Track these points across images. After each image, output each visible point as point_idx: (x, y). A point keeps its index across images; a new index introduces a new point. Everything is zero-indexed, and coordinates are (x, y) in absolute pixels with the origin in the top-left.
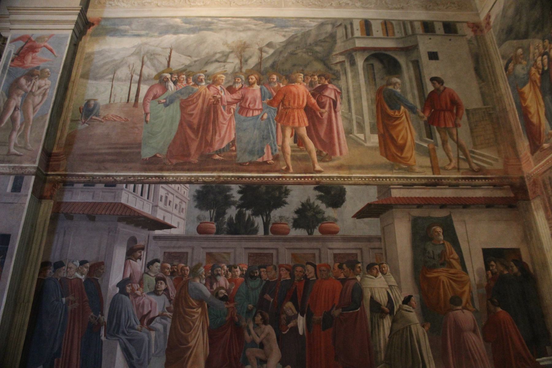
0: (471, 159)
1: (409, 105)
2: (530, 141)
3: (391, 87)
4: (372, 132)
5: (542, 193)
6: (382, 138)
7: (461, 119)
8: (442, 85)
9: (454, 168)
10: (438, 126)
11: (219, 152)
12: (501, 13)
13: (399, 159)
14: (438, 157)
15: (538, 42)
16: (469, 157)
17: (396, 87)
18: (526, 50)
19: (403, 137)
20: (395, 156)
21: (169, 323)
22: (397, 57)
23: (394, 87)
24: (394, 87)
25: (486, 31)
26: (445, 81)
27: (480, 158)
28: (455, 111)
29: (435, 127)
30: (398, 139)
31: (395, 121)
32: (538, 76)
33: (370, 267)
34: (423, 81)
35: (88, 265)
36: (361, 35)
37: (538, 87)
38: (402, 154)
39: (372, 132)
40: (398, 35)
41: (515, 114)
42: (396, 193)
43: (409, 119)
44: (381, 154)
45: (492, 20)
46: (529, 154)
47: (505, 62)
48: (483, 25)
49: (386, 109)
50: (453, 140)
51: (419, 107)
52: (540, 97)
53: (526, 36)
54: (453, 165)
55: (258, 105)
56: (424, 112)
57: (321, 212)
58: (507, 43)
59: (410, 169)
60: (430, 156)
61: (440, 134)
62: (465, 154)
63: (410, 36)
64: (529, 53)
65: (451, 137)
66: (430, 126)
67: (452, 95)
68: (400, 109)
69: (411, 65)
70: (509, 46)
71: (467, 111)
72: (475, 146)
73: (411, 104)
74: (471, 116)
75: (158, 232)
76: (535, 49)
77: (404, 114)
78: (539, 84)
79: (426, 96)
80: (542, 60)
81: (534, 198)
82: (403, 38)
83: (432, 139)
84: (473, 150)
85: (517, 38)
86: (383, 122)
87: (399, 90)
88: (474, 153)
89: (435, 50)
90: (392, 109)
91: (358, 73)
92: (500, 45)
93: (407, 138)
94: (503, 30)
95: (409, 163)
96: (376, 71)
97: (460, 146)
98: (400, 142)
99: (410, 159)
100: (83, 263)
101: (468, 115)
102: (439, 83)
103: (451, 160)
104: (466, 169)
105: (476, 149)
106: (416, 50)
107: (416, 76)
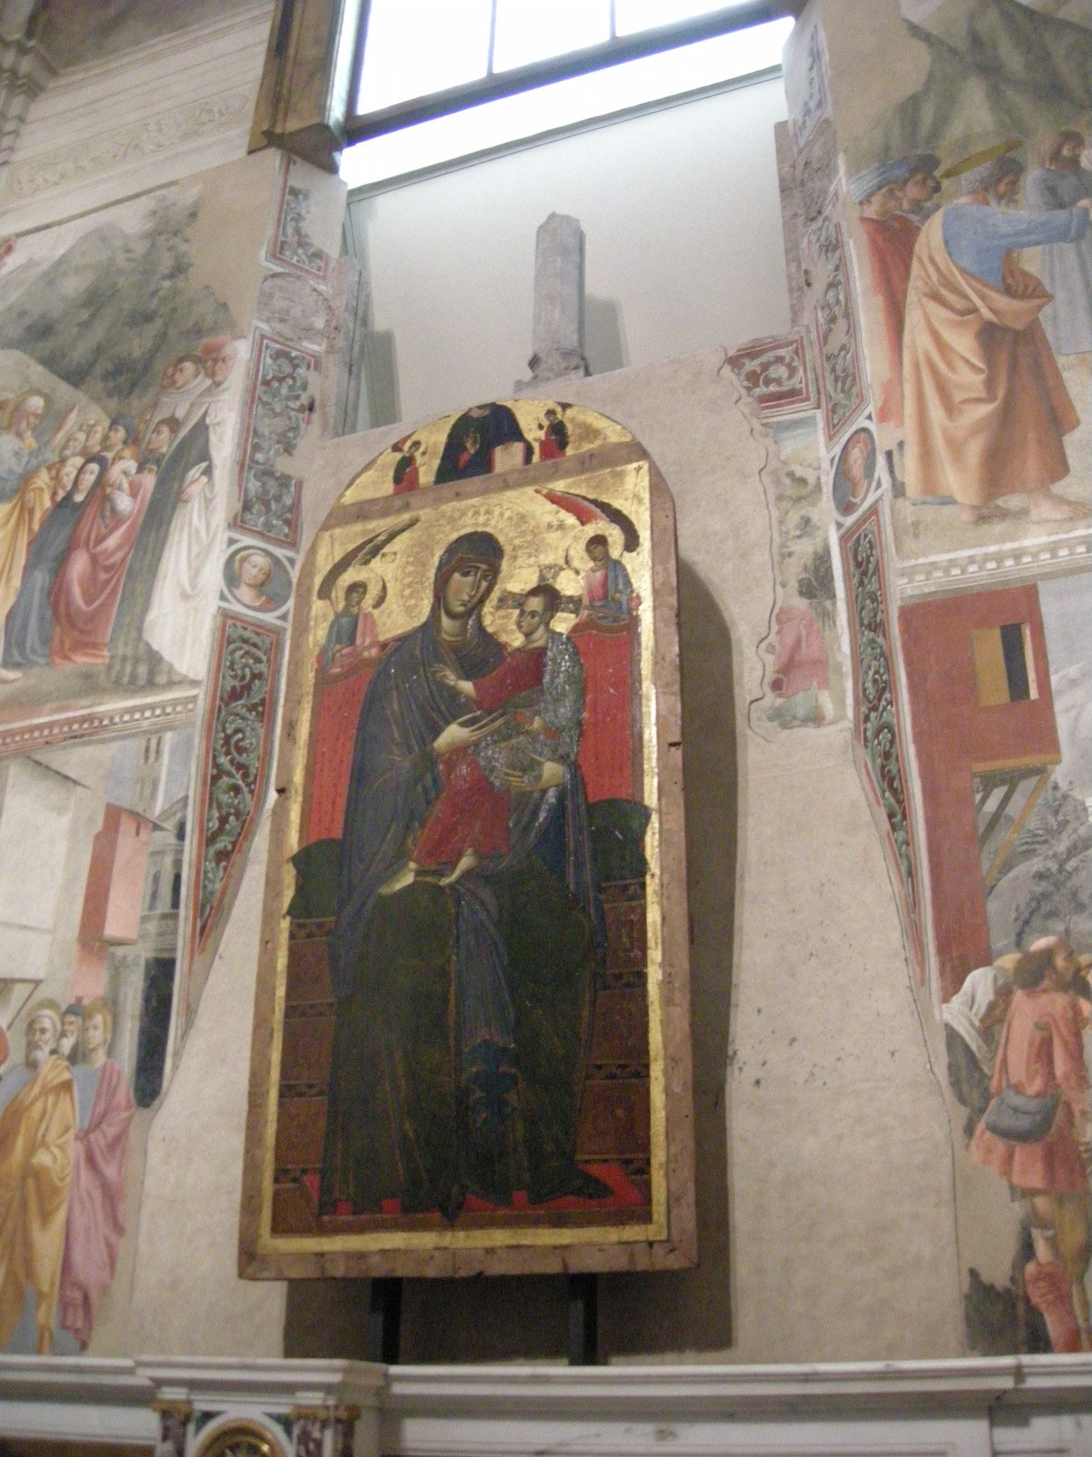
12: (45, 267)
15: (97, 416)
18: (54, 416)
32: (48, 504)
37: (30, 530)
53: (76, 378)
58: (17, 354)
64: (59, 428)
76: (80, 429)
78: (36, 526)
80: (81, 471)
85: (49, 362)
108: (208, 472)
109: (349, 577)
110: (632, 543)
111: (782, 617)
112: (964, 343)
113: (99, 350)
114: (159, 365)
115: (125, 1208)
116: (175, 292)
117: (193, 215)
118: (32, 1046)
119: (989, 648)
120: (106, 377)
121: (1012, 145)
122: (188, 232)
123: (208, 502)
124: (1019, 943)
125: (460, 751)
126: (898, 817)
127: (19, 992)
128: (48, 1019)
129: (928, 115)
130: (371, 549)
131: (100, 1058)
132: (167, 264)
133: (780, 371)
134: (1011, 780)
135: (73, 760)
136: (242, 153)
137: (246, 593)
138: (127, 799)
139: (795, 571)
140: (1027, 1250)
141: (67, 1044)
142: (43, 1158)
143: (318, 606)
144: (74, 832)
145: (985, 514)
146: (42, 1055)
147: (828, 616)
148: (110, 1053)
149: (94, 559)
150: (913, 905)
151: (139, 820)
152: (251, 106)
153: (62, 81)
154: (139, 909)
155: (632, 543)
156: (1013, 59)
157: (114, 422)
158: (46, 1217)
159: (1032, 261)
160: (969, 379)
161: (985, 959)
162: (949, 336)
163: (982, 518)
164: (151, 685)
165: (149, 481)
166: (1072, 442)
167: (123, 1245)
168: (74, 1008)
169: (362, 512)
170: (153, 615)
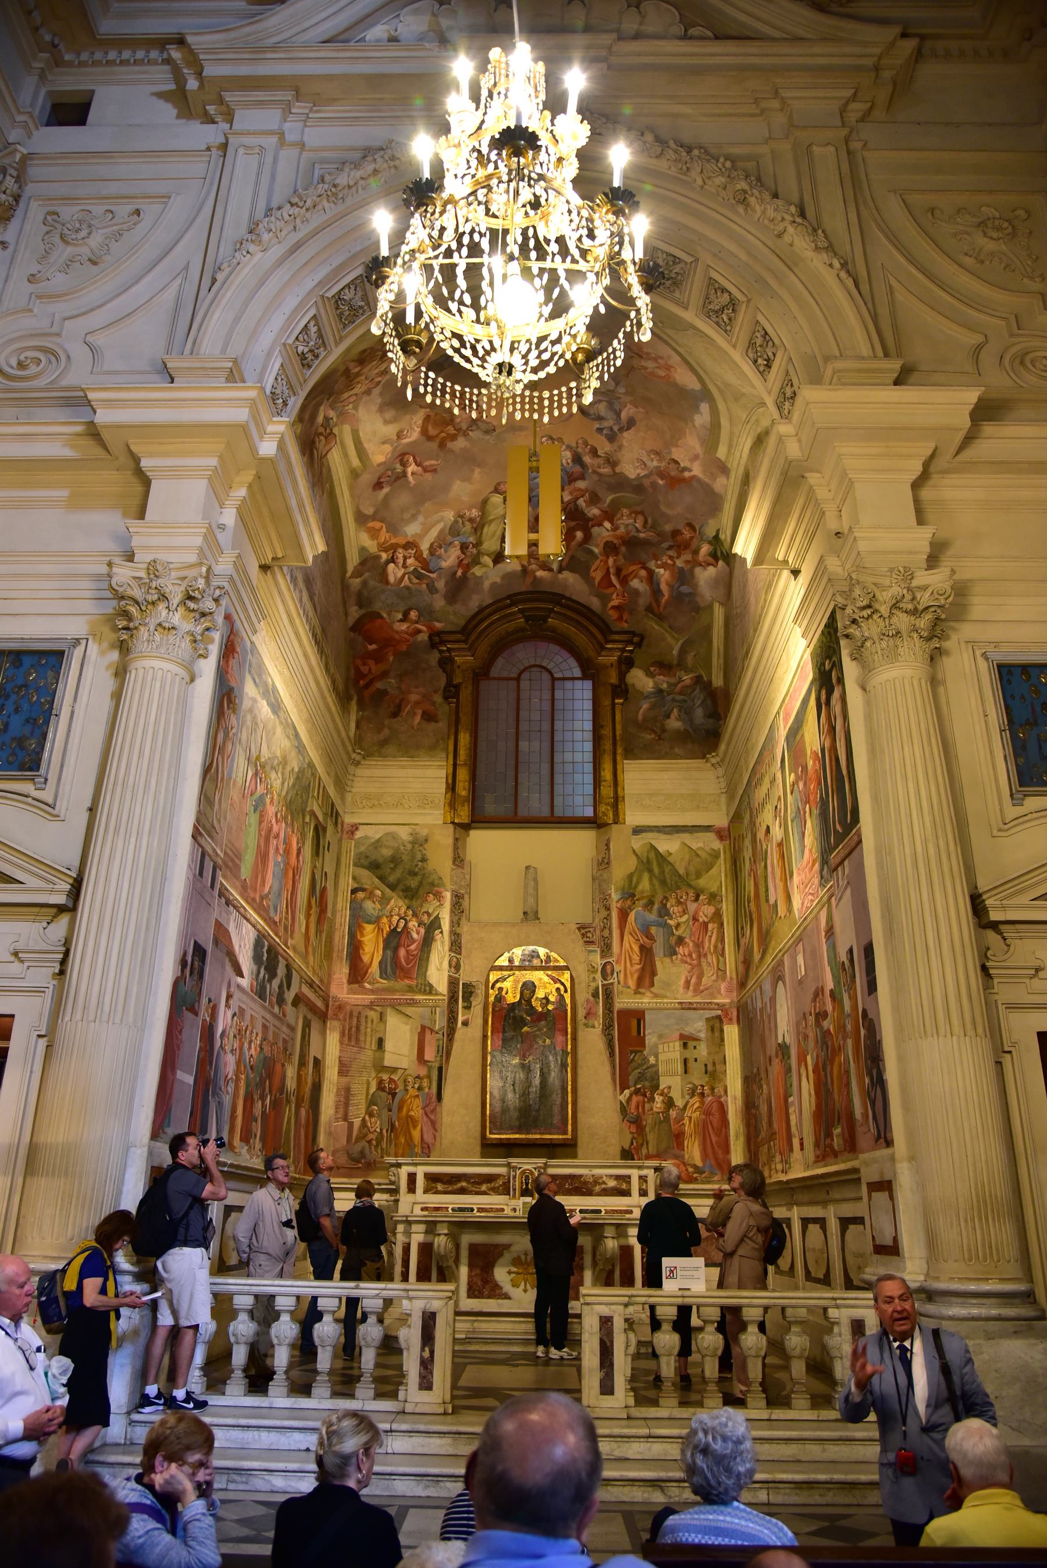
2: (350, 970)
5: (345, 1020)
11: (267, 896)
12: (373, 840)
21: (233, 1085)
25: (345, 836)
33: (290, 1054)
35: (211, 1004)
41: (343, 936)
42: (305, 990)
45: (359, 834)
46: (345, 981)
47: (356, 886)
48: (346, 828)
52: (381, 946)
53: (392, 887)
55: (281, 851)
57: (284, 992)
59: (307, 964)
70: (368, 878)
75: (239, 979)
81: (332, 1019)
85: (382, 878)
92: (355, 865)
94: (367, 857)
100: (210, 1001)
108: (441, 932)
109: (498, 985)
110: (566, 991)
111: (588, 1001)
112: (636, 948)
113: (399, 881)
114: (421, 892)
115: (437, 1126)
116: (424, 868)
117: (426, 840)
118: (406, 1086)
119: (634, 1023)
120: (403, 891)
121: (653, 896)
122: (426, 846)
123: (443, 943)
124: (635, 1085)
125: (528, 1033)
126: (612, 1054)
127: (400, 1072)
128: (410, 1079)
129: (635, 879)
130: (504, 979)
131: (427, 1090)
132: (419, 857)
133: (589, 935)
134: (636, 1052)
135: (409, 1010)
136: (441, 822)
137: (453, 969)
138: (428, 1024)
139: (591, 990)
140: (632, 1143)
141: (416, 1086)
142: (412, 1113)
143: (491, 991)
144: (411, 1030)
145: (636, 992)
146: (409, 1088)
147: (598, 1003)
148: (429, 1088)
149: (407, 951)
150: (614, 1074)
151: (432, 1030)
152: (442, 804)
153: (366, 762)
154: (434, 1054)
155: (566, 991)
156: (656, 870)
157: (408, 908)
158: (415, 1127)
159: (653, 930)
160: (636, 958)
161: (628, 1088)
162: (633, 946)
163: (635, 993)
164: (430, 993)
165: (422, 931)
166: (656, 978)
167: (437, 1135)
168: (418, 1077)
169: (501, 968)
170: (429, 973)
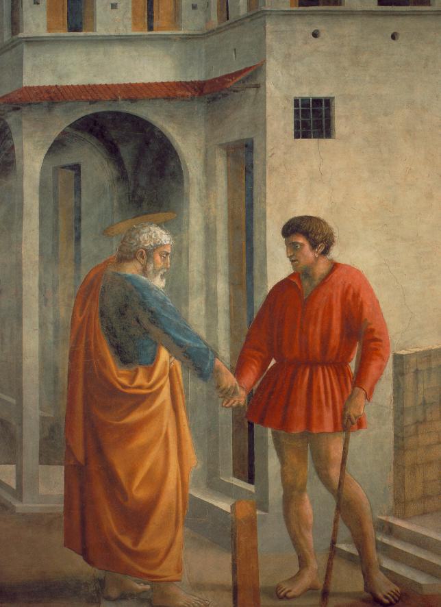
0: (374, 555)
1: (188, 341)
3: (131, 269)
4: (46, 458)
6: (78, 478)
7: (368, 397)
8: (325, 252)
9: (311, 590)
10: (284, 425)
13: (125, 558)
14: (262, 547)
16: (372, 547)
17: (150, 267)
19: (150, 471)
20: (114, 546)
22: (172, 131)
23: (144, 271)
24: (144, 271)
26: (337, 234)
27: (410, 550)
28: (352, 366)
29: (269, 431)
30: (130, 482)
31: (130, 410)
34: (256, 236)
36: (49, 29)
38: (136, 543)
39: (46, 458)
40: (191, 23)
43: (180, 398)
44: (68, 544)
49: (104, 362)
50: (325, 479)
51: (224, 350)
54: (306, 580)
56: (238, 371)
60: (234, 548)
61: (283, 462)
62: (360, 540)
63: (240, 22)
65: (318, 471)
66: (251, 425)
67: (356, 296)
68: (154, 359)
69: (221, 164)
71: (399, 360)
72: (401, 505)
73: (198, 338)
74: (409, 379)
77: (166, 381)
79: (259, 300)
82: (212, 32)
83: (251, 479)
84: (391, 520)
86: (87, 416)
87: (159, 283)
88: (390, 530)
89: (322, 93)
90: (125, 358)
91: (21, 205)
93: (165, 476)
95: (156, 572)
96: (85, 198)
97: (345, 508)
98: (139, 493)
99: (161, 562)
101: (399, 374)
102: (314, 246)
103: (303, 562)
104: (348, 595)
105: (404, 518)
106: (252, 92)
107: (232, 217)
